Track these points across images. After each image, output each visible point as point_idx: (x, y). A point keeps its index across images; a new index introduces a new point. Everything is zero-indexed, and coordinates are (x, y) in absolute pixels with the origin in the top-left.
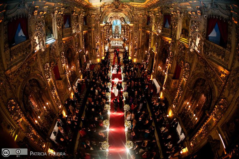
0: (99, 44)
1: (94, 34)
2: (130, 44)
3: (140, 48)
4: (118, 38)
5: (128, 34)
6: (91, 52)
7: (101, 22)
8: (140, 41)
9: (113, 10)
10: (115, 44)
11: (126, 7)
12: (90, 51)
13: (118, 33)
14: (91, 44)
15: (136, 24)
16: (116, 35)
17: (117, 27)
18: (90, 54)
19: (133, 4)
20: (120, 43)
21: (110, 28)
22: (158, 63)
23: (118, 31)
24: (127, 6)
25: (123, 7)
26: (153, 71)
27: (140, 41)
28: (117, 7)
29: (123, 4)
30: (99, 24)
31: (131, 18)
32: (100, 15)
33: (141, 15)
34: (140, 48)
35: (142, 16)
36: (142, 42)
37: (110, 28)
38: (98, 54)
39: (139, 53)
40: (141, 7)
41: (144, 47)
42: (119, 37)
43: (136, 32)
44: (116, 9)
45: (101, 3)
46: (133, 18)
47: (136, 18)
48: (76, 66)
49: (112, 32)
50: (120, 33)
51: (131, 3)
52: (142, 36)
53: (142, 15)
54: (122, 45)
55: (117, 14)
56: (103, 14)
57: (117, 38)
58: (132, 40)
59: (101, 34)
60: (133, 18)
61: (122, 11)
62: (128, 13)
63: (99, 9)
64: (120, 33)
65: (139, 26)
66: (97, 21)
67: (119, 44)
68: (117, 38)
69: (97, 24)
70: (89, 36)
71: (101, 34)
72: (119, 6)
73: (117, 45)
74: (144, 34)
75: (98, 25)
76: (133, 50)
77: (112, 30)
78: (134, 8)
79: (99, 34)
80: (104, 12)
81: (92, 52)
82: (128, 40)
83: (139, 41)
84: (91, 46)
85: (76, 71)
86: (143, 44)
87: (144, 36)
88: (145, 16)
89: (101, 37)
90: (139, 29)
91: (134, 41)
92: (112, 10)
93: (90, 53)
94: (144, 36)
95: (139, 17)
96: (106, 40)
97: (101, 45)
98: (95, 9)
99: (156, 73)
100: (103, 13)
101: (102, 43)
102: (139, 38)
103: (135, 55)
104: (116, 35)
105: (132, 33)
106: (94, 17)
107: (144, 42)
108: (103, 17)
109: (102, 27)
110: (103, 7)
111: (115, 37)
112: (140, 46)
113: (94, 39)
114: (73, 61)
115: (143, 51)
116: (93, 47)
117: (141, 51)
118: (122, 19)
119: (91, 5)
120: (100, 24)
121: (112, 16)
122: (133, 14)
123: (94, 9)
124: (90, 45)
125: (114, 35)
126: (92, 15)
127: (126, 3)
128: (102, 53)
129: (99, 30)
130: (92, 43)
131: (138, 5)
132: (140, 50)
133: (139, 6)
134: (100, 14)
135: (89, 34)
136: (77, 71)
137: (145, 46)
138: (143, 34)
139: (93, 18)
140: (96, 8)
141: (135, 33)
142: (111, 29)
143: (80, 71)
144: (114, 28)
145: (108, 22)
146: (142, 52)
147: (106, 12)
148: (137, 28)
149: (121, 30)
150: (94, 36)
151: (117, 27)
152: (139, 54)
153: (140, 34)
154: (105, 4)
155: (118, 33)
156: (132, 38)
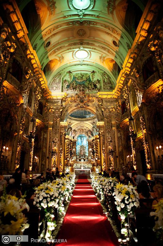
0: (57, 151)
1: (50, 135)
2: (102, 151)
3: (117, 157)
4: (85, 161)
5: (98, 148)
6: (43, 163)
7: (62, 120)
8: (117, 145)
9: (77, 105)
10: (80, 168)
11: (93, 101)
12: (42, 161)
13: (84, 154)
14: (44, 150)
15: (108, 122)
16: (81, 156)
17: (82, 147)
18: (40, 165)
19: (102, 95)
20: (87, 167)
21: (73, 146)
22: (152, 145)
23: (84, 152)
24: (94, 99)
25: (89, 101)
26: (148, 166)
27: (117, 145)
28: (82, 101)
29: (89, 97)
30: (59, 123)
31: (100, 114)
32: (61, 110)
33: (113, 109)
34: (117, 157)
35: (114, 110)
36: (119, 147)
37: (73, 146)
38: (54, 167)
39: (116, 165)
40: (111, 98)
41: (124, 152)
42: (86, 160)
43: (109, 132)
44: (81, 104)
45: (62, 93)
46: (103, 114)
47: (106, 113)
48: (13, 153)
49: (75, 153)
50: (87, 154)
51: (99, 93)
52: (118, 138)
53: (114, 108)
54: (89, 170)
55: (82, 123)
56: (65, 109)
57: (82, 160)
58: (104, 146)
59: (61, 136)
60: (103, 114)
61: (89, 106)
62: (96, 108)
63: (59, 104)
64: (87, 154)
65: (111, 123)
66: (57, 118)
67: (85, 168)
68: (82, 160)
69: (56, 122)
70: (43, 137)
71: (61, 136)
72: (85, 98)
73: (82, 169)
74: (121, 134)
75: (58, 123)
76: (107, 160)
77: (76, 149)
78: (103, 101)
79: (57, 135)
80: (66, 108)
81: (45, 162)
82: (98, 159)
83: (115, 146)
84: (44, 153)
85: (10, 159)
86: (120, 149)
87: (121, 136)
88: (118, 107)
89: (61, 141)
90: (112, 127)
91: (107, 147)
92: (75, 105)
93: (42, 164)
94: (121, 136)
95: (110, 112)
96: (67, 159)
97: (60, 153)
98: (55, 102)
99: (156, 166)
100: (64, 108)
101: (62, 150)
102: (115, 142)
103: (111, 168)
104: (81, 156)
105: (104, 136)
106: (54, 113)
107: (122, 145)
108: (64, 114)
109: (62, 127)
110: (65, 101)
111: (80, 160)
112: (117, 153)
113: (50, 142)
114: (11, 141)
115: (123, 160)
116: (48, 156)
117: (120, 161)
118: (89, 133)
119: (50, 95)
120: (61, 123)
121: (76, 129)
122: (103, 108)
123: (53, 101)
124: (43, 151)
125: (78, 157)
126: (50, 108)
127: (93, 94)
128: (60, 166)
129: (59, 130)
130: (46, 148)
131: (107, 95)
132: (118, 159)
133: (109, 97)
134: (61, 108)
135: (44, 135)
136: (11, 161)
137: (124, 150)
138: (119, 135)
139: (52, 113)
140: (56, 101)
141: (107, 135)
142: (74, 146)
143: (18, 167)
144: (78, 148)
145: (71, 126)
146: (122, 162)
147: (68, 108)
148: (109, 126)
149: (89, 149)
150: (50, 138)
151: (82, 147)
152: (118, 167)
153: (114, 134)
154: (68, 97)
155: (85, 156)
156: (104, 143)
